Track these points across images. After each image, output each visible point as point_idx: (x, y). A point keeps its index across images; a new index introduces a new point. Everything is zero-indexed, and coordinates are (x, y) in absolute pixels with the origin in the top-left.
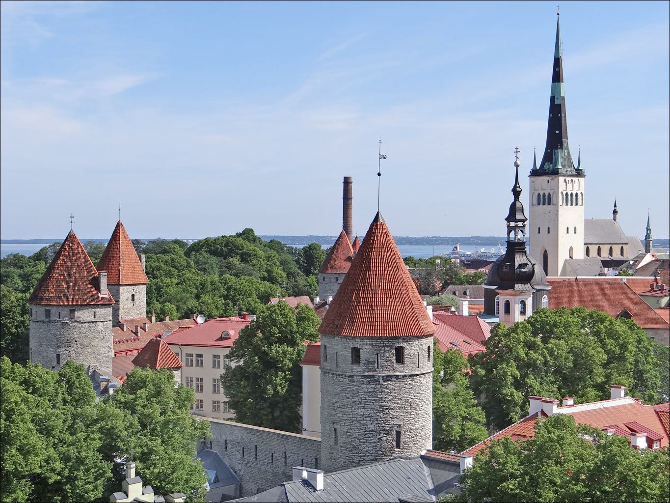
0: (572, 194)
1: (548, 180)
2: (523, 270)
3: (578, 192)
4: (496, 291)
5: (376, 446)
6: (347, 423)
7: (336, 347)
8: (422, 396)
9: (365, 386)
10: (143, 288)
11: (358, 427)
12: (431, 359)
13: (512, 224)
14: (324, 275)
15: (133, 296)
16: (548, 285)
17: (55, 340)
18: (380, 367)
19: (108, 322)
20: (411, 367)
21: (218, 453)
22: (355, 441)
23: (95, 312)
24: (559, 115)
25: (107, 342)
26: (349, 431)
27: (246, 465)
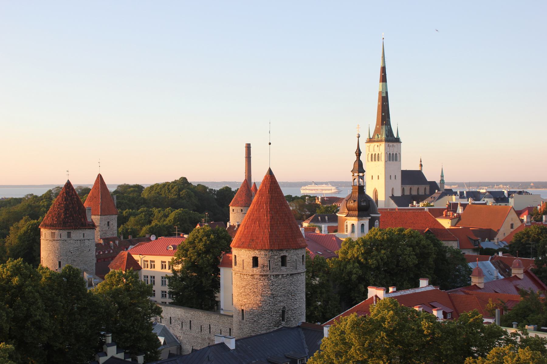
0: (393, 154)
1: (378, 145)
2: (362, 204)
3: (397, 153)
4: (346, 218)
5: (269, 320)
7: (242, 256)
8: (299, 287)
9: (262, 282)
10: (115, 217)
11: (257, 308)
12: (305, 263)
13: (356, 174)
14: (234, 208)
15: (108, 222)
16: (379, 214)
17: (58, 252)
18: (271, 269)
19: (93, 240)
20: (291, 269)
21: (166, 326)
22: (255, 317)
23: (84, 234)
24: (384, 103)
25: (92, 253)
26: (251, 311)
27: (184, 333)
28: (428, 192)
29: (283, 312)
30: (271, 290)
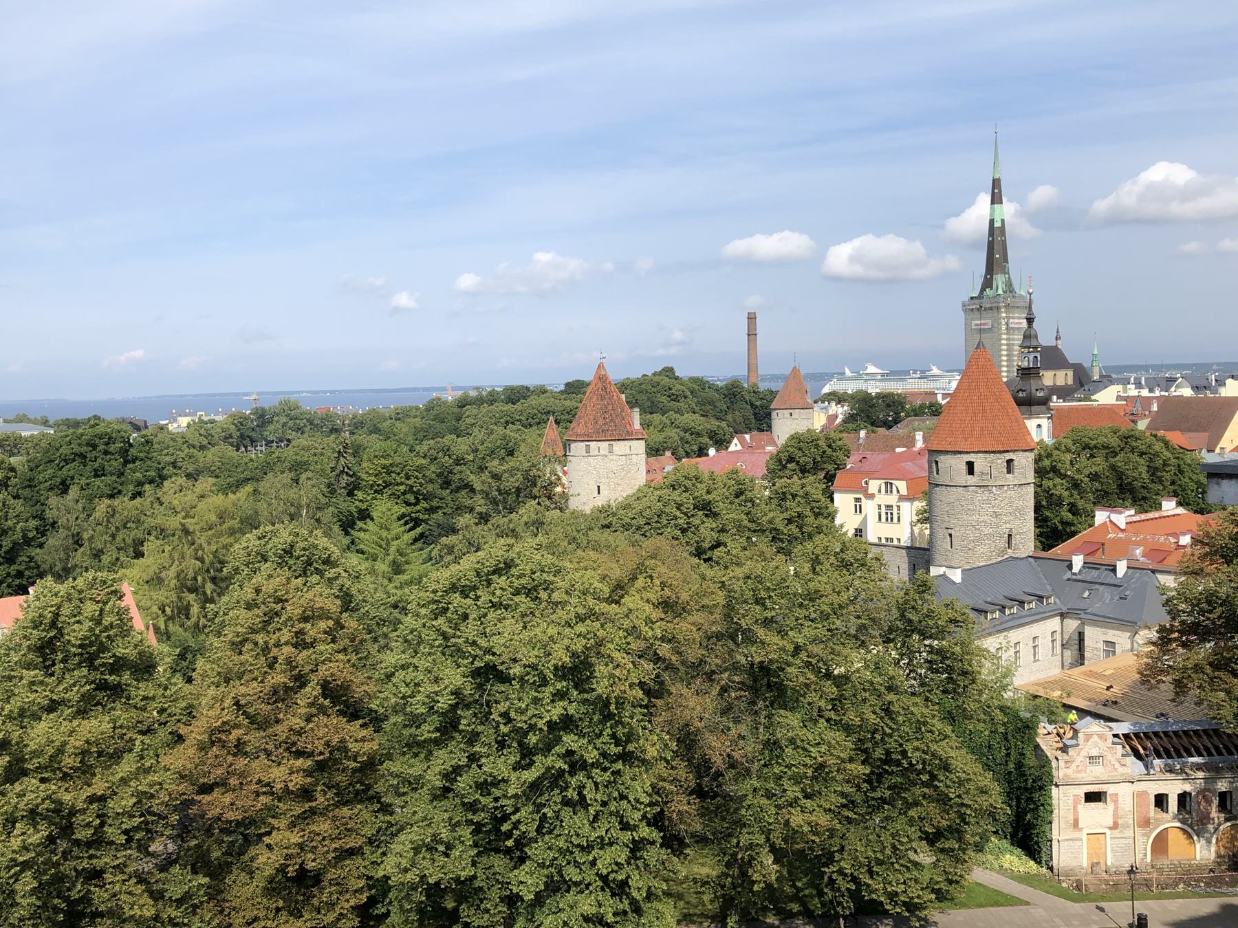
2: (1039, 395)
6: (963, 528)
28: (1070, 382)
29: (1010, 536)
30: (993, 506)
